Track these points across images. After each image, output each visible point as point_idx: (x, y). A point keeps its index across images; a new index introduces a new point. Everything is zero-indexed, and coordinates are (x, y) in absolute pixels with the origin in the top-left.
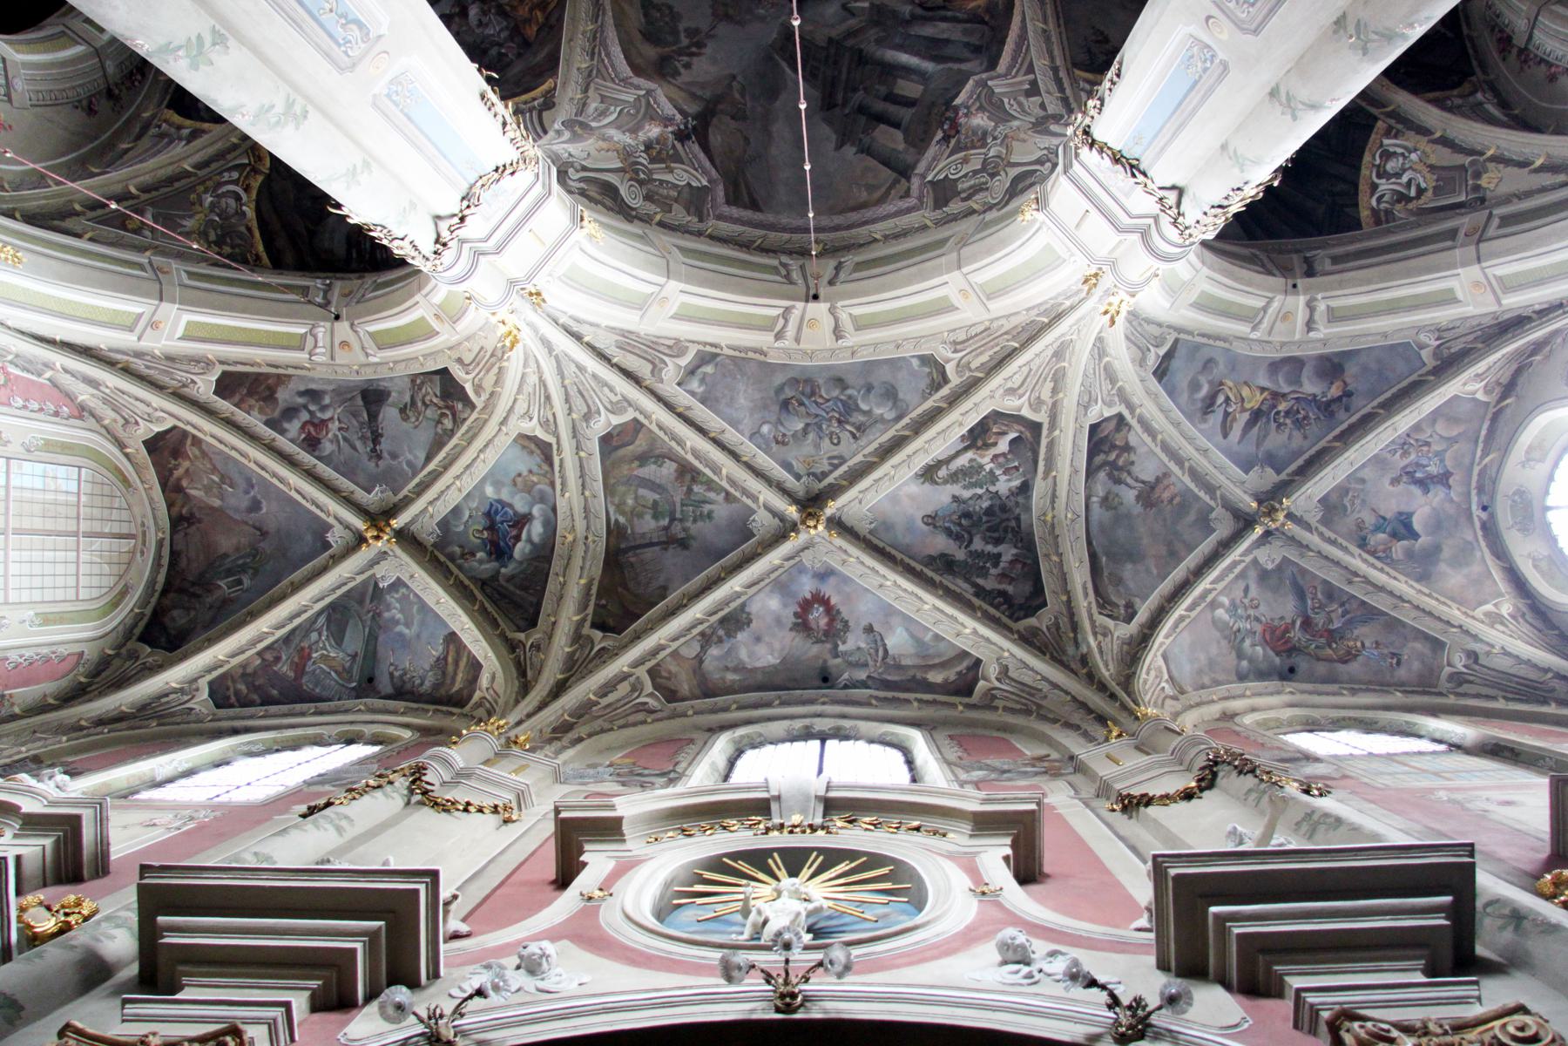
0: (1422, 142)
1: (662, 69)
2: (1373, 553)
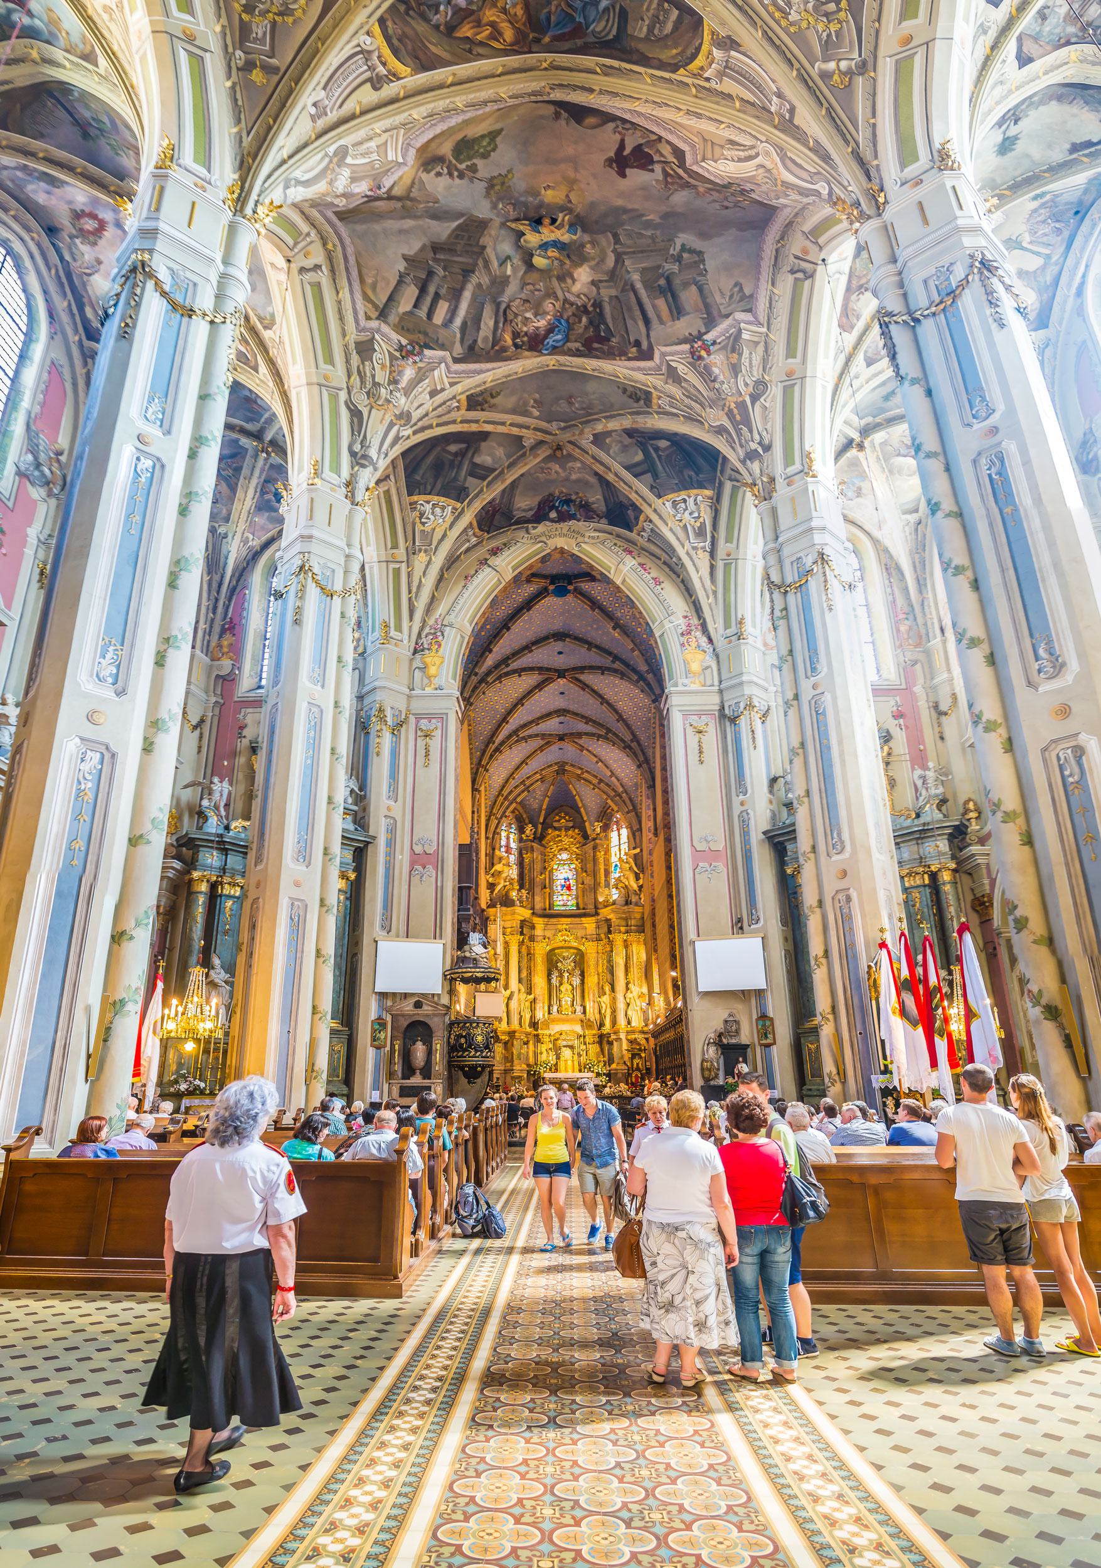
0: (447, 525)
1: (430, 160)
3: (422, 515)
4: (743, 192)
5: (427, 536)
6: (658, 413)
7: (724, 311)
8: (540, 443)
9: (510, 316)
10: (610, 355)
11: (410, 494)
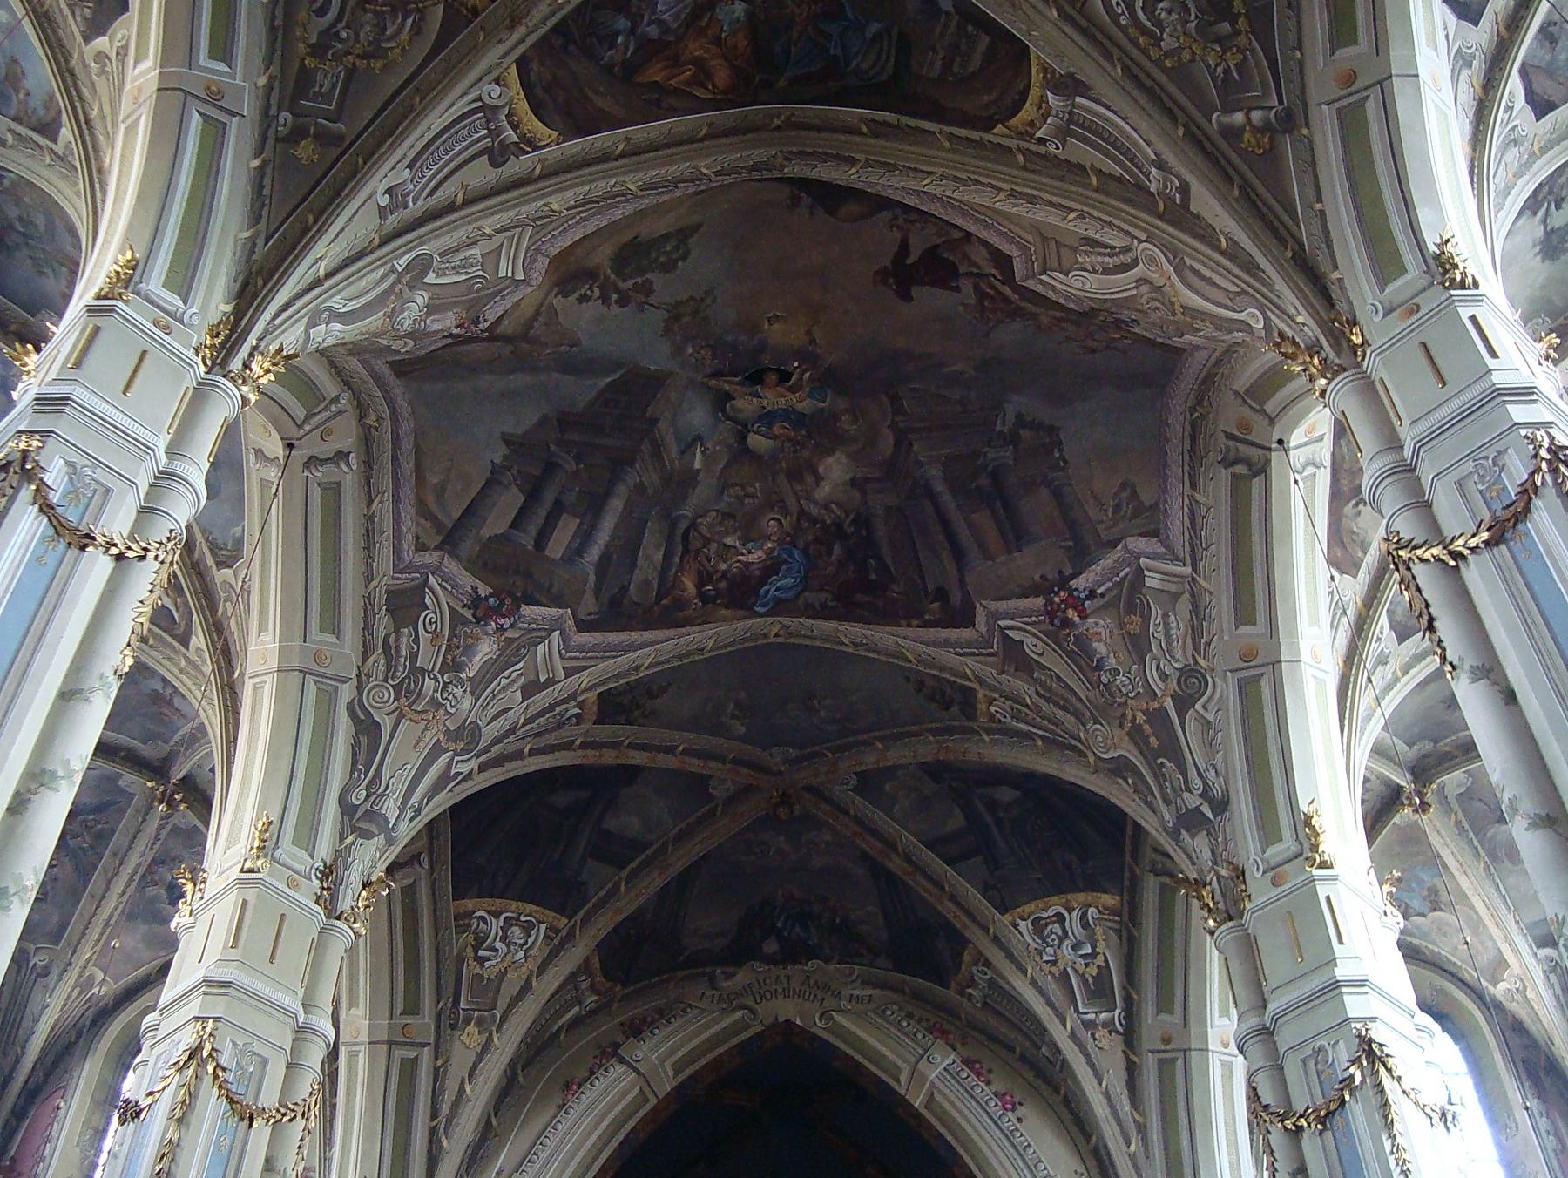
0: (533, 965)
1: (570, 274)
2: (149, 870)
3: (479, 942)
4: (1118, 323)
5: (487, 989)
6: (989, 732)
7: (1105, 536)
8: (746, 791)
9: (696, 544)
10: (888, 616)
11: (459, 895)
